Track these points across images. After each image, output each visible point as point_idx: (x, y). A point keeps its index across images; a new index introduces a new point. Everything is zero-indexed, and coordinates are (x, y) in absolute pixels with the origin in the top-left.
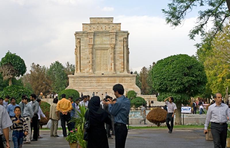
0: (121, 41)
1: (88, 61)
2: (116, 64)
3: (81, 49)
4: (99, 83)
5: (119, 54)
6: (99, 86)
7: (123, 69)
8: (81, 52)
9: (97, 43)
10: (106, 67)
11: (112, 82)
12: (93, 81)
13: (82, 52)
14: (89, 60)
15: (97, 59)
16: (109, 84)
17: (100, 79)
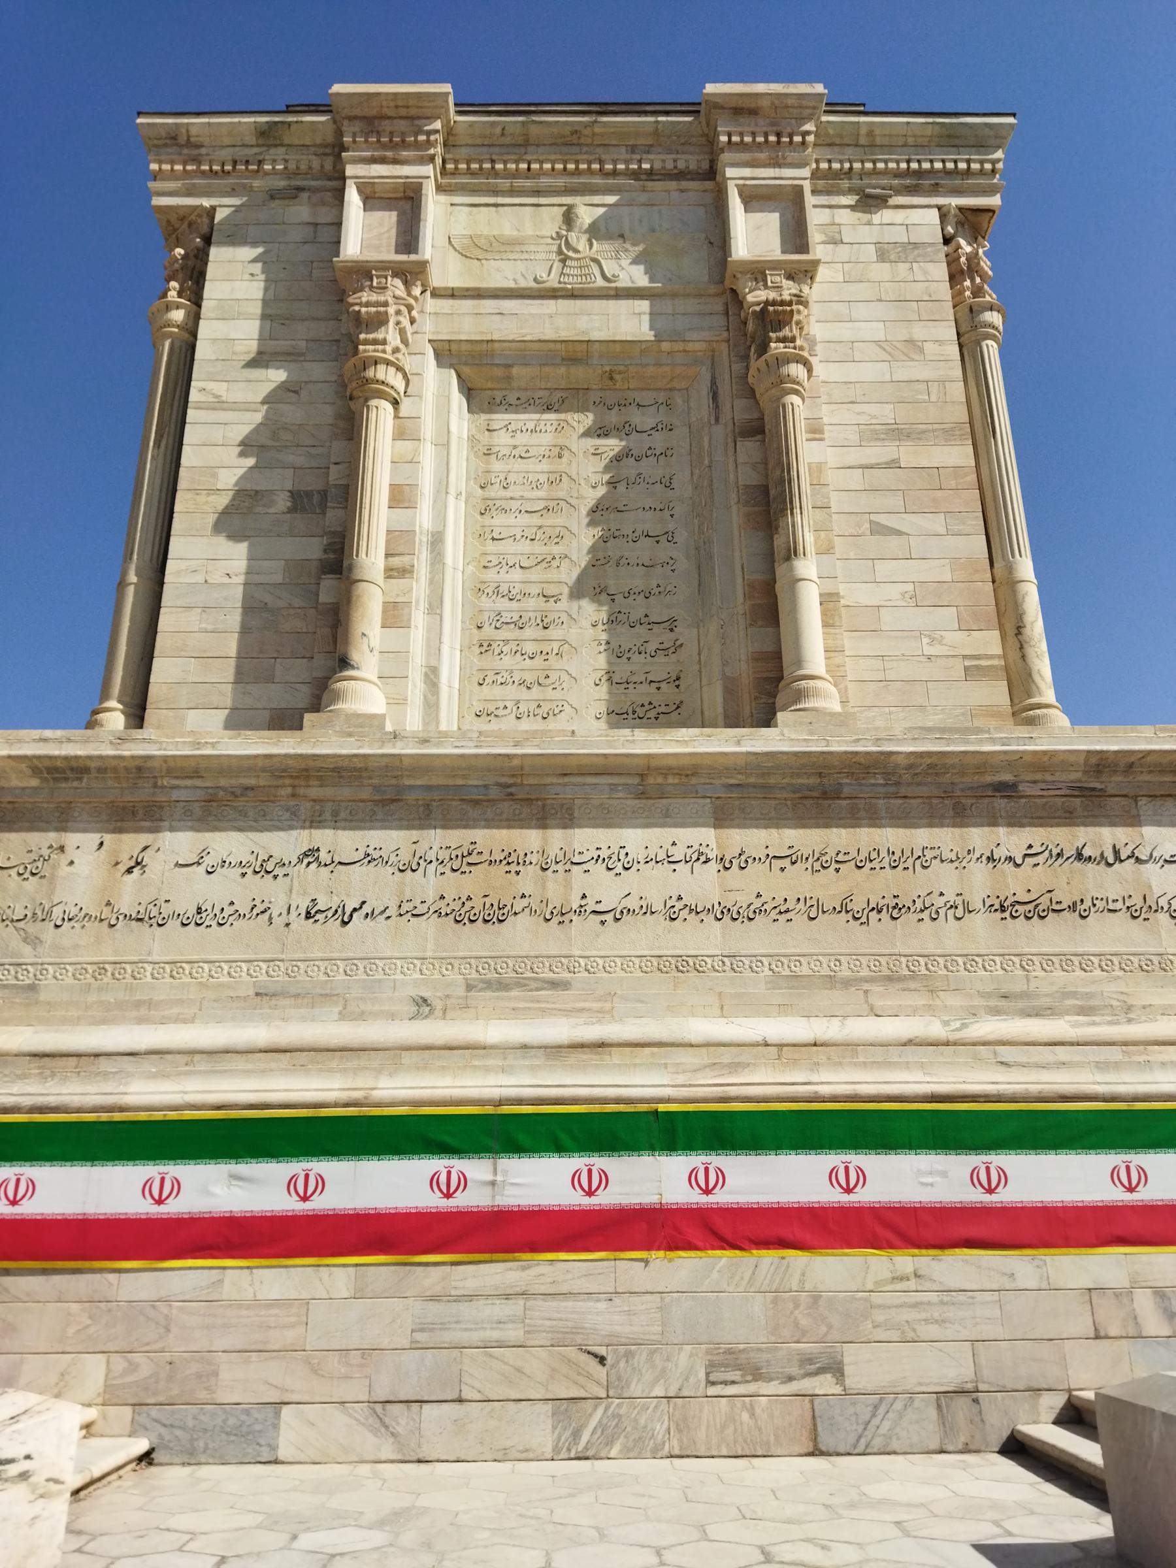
0: (910, 250)
1: (313, 549)
2: (855, 594)
3: (202, 351)
4: (497, 916)
5: (897, 433)
6: (502, 986)
7: (997, 694)
8: (194, 396)
9: (503, 273)
10: (662, 668)
11: (815, 910)
12: (358, 885)
13: (218, 404)
14: (333, 515)
15: (499, 520)
16: (757, 939)
17: (529, 839)
